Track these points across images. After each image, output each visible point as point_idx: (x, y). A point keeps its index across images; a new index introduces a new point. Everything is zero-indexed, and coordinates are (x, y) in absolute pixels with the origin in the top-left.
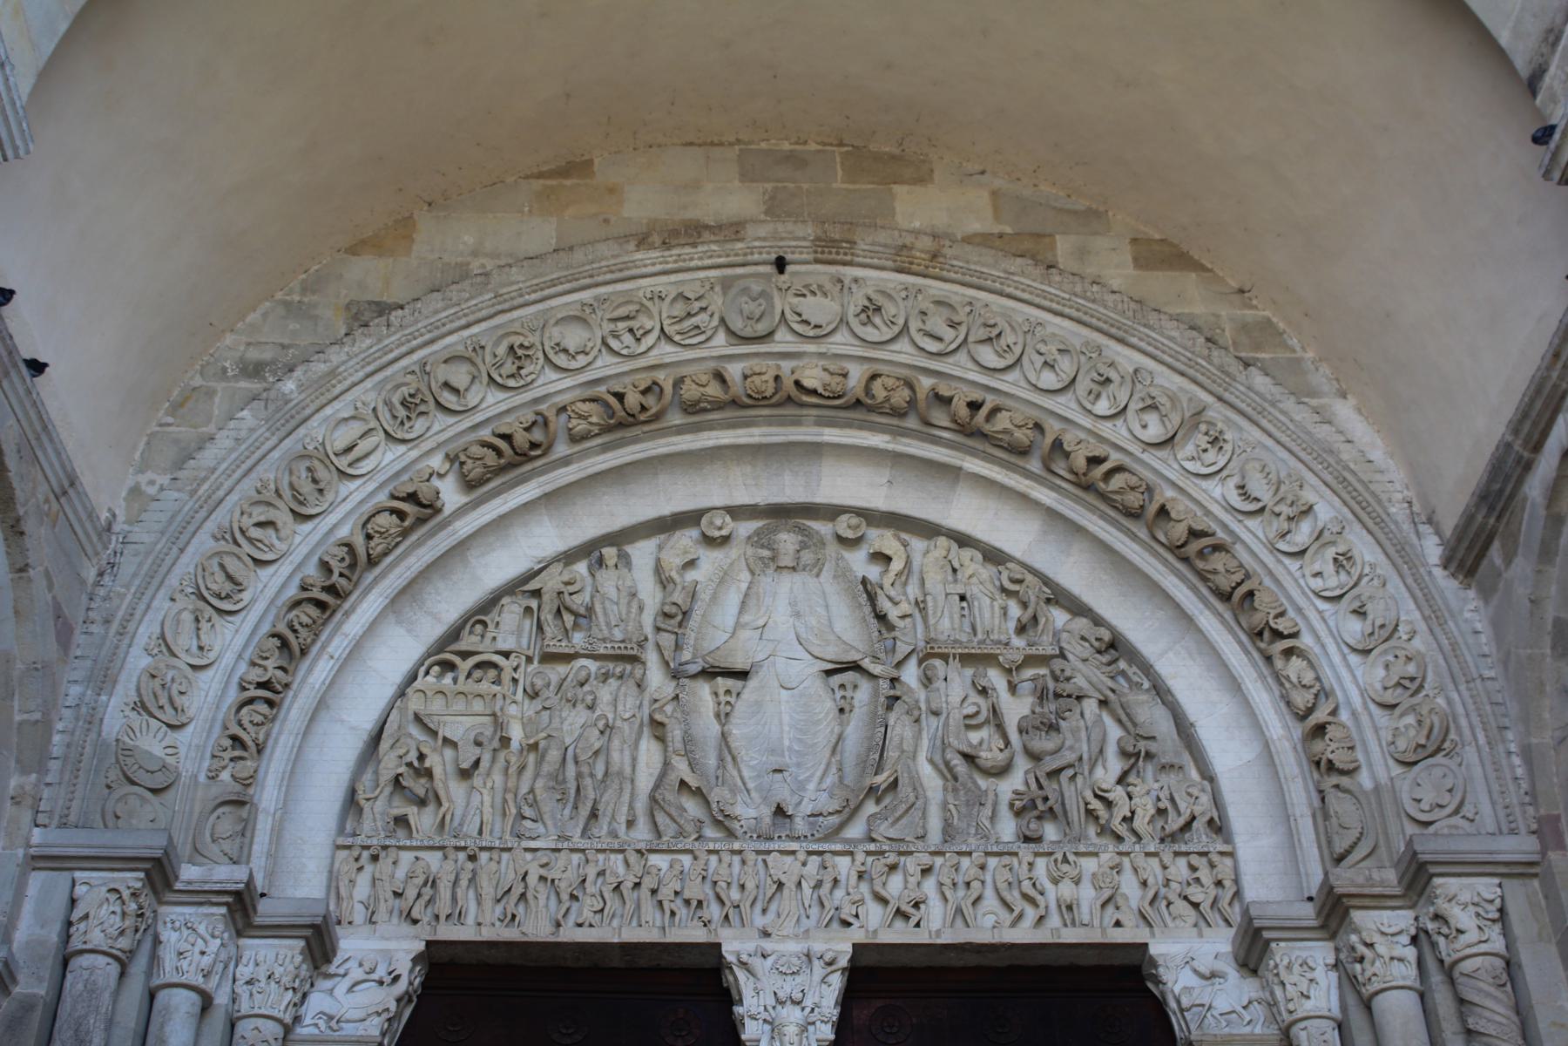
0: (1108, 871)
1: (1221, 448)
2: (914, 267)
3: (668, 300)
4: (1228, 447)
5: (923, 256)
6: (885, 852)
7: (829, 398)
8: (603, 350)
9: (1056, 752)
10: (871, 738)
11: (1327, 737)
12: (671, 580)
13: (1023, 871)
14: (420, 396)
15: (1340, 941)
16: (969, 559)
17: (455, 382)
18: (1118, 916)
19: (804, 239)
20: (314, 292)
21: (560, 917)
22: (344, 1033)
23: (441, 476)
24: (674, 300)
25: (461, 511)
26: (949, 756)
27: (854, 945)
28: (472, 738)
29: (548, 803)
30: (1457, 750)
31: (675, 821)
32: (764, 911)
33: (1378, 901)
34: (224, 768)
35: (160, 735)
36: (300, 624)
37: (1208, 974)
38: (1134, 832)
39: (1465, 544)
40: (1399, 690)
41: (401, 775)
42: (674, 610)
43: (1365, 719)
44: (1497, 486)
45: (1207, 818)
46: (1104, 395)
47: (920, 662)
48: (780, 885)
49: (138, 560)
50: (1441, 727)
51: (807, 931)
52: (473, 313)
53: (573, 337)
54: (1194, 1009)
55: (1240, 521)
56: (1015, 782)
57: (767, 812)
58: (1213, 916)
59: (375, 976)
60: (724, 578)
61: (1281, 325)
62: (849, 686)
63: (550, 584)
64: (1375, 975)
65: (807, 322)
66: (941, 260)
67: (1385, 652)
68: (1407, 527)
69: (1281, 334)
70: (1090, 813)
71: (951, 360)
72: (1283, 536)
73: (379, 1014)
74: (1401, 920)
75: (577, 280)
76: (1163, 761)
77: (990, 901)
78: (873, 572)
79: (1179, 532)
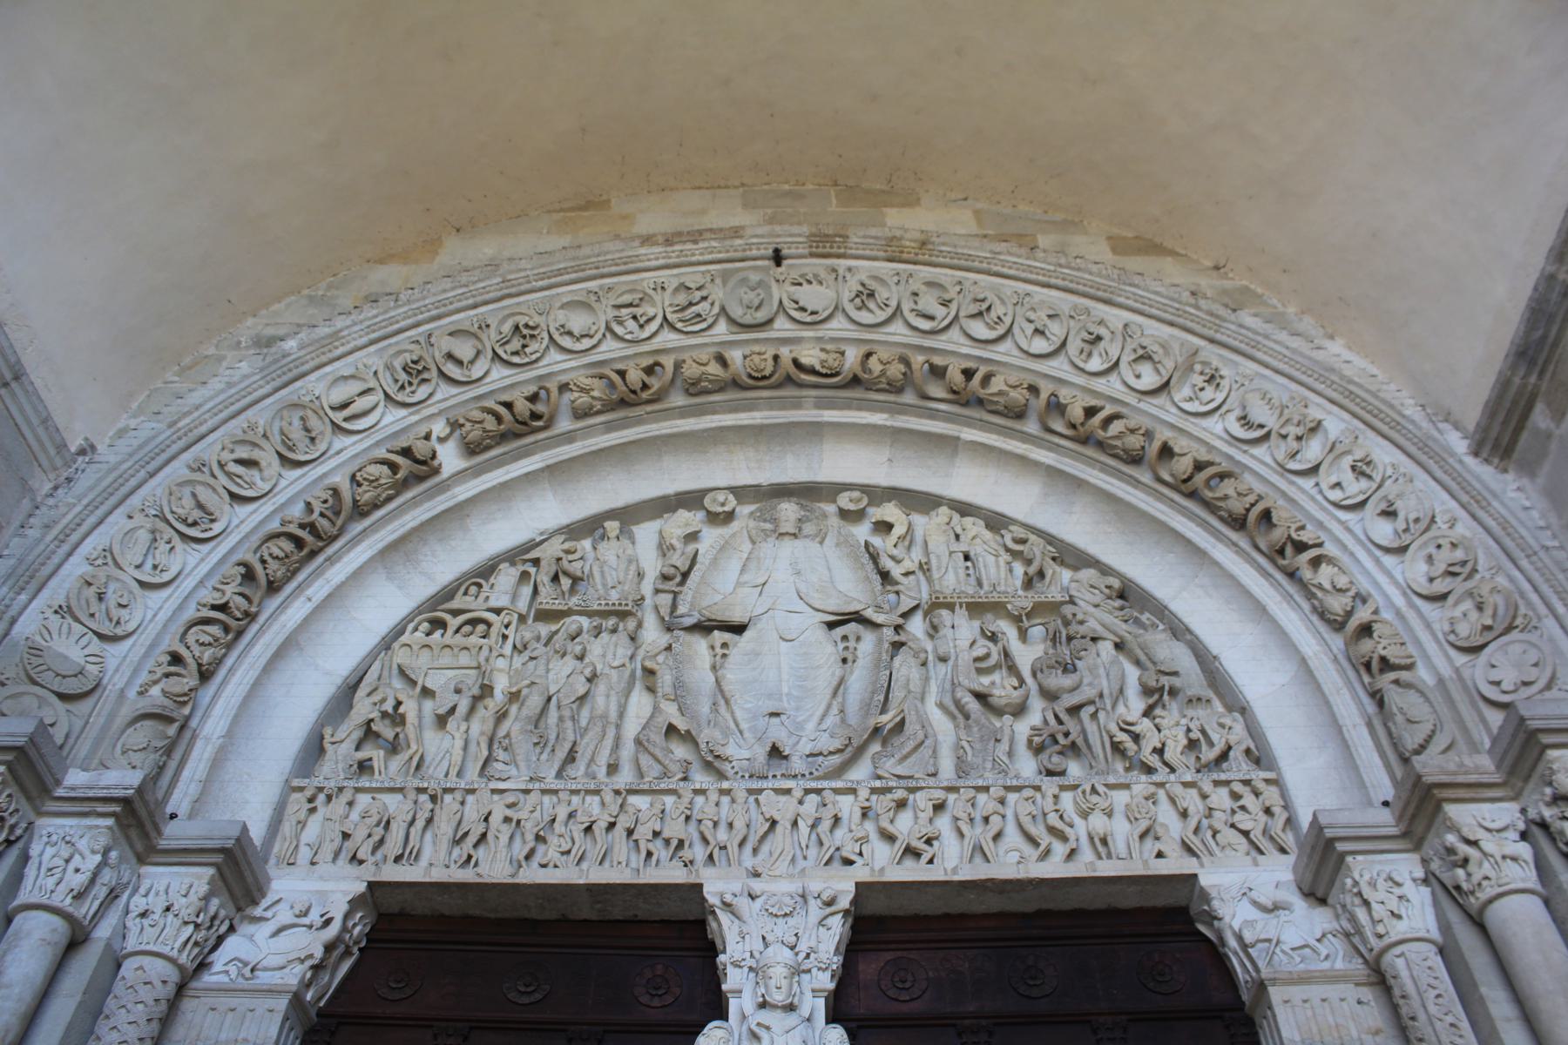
0: (1143, 801)
1: (1218, 385)
2: (905, 256)
3: (669, 291)
4: (1225, 383)
5: (913, 244)
6: (892, 788)
7: (826, 376)
8: (608, 335)
9: (1074, 689)
10: (874, 683)
11: (1375, 635)
12: (673, 547)
13: (1049, 804)
14: (423, 363)
15: (1428, 850)
16: (973, 526)
17: (458, 353)
18: (1158, 846)
19: (800, 235)
20: (337, 289)
21: (521, 857)
22: (258, 981)
23: (441, 440)
24: (677, 290)
25: (460, 476)
26: (959, 695)
27: (857, 884)
28: (452, 687)
29: (523, 746)
30: (1533, 623)
31: (659, 762)
32: (755, 851)
33: (1474, 791)
34: (156, 682)
35: (84, 641)
36: (271, 555)
37: (1270, 905)
38: (1166, 764)
39: (1501, 417)
40: (1449, 579)
41: (372, 720)
42: (672, 571)
43: (1411, 616)
44: (1538, 334)
45: (1244, 747)
46: (1095, 353)
47: (926, 615)
48: (774, 823)
49: (98, 476)
50: (1507, 609)
51: (803, 870)
52: (482, 294)
53: (578, 321)
54: (1260, 945)
55: (1245, 452)
56: (1034, 717)
57: (761, 752)
58: (1264, 844)
59: (306, 921)
60: (724, 547)
61: (1259, 290)
62: (852, 638)
63: (549, 552)
64: (1487, 878)
65: (803, 309)
66: (930, 247)
67: (1425, 544)
68: (1425, 424)
69: (1260, 296)
70: (1117, 748)
71: (944, 337)
72: (1293, 456)
73: (302, 961)
74: (1505, 813)
75: (583, 270)
76: (1189, 693)
77: (1012, 836)
78: (877, 541)
79: (1183, 465)
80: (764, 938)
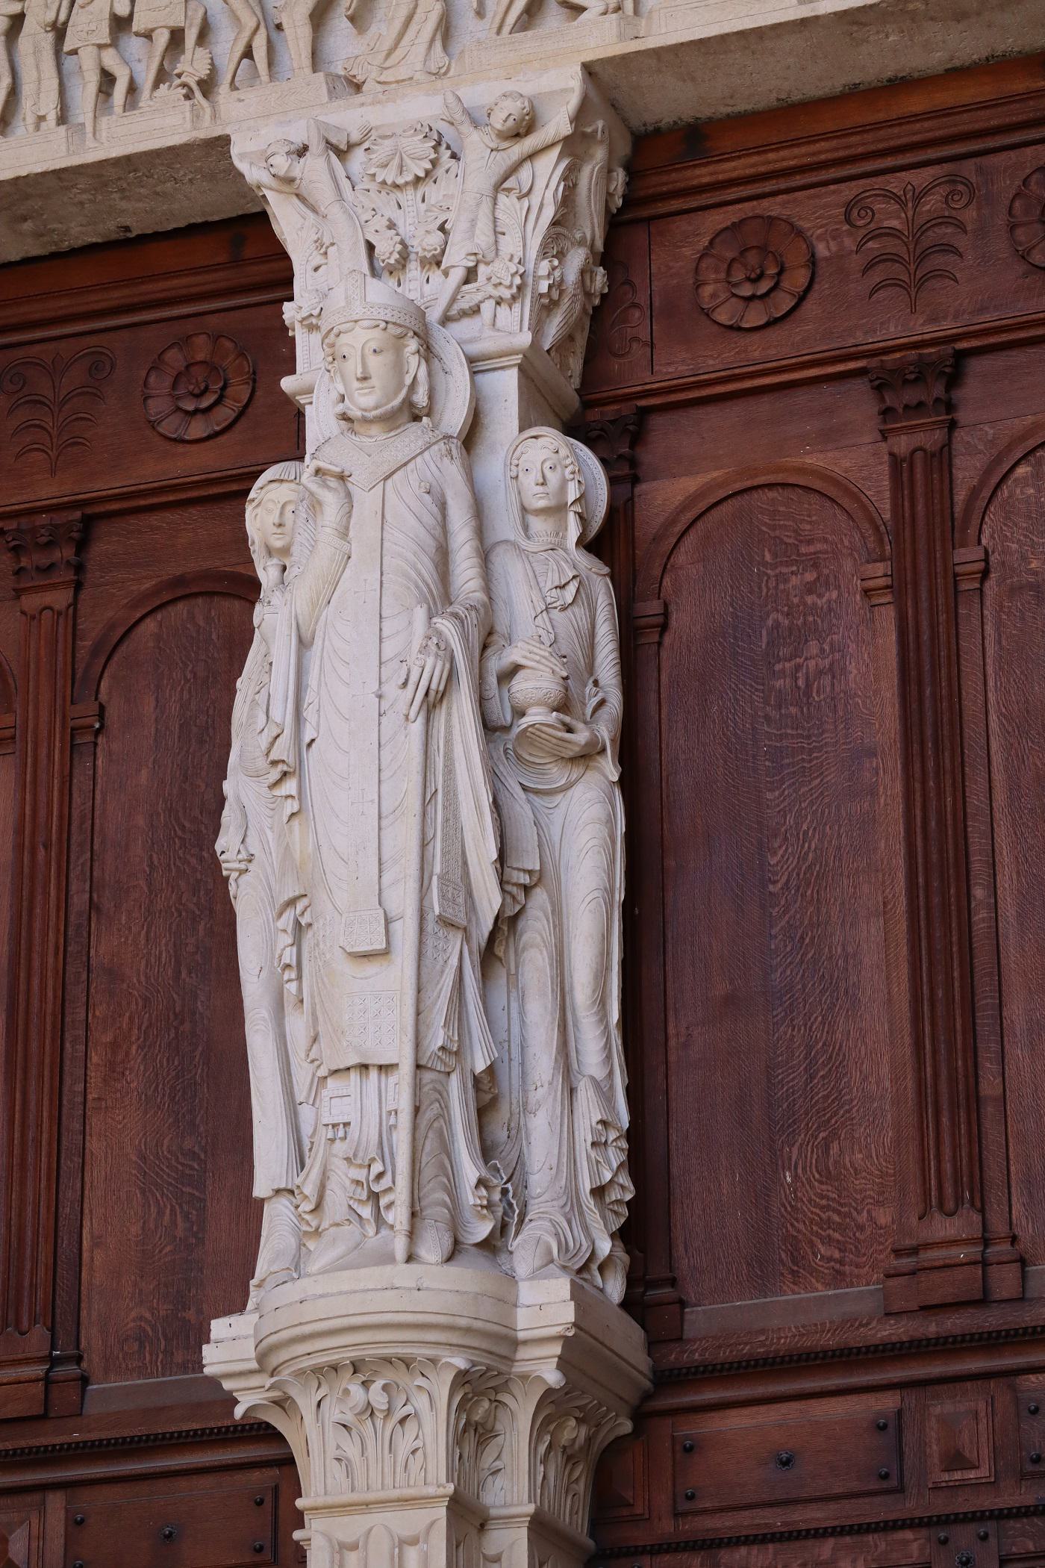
80: (371, 247)
